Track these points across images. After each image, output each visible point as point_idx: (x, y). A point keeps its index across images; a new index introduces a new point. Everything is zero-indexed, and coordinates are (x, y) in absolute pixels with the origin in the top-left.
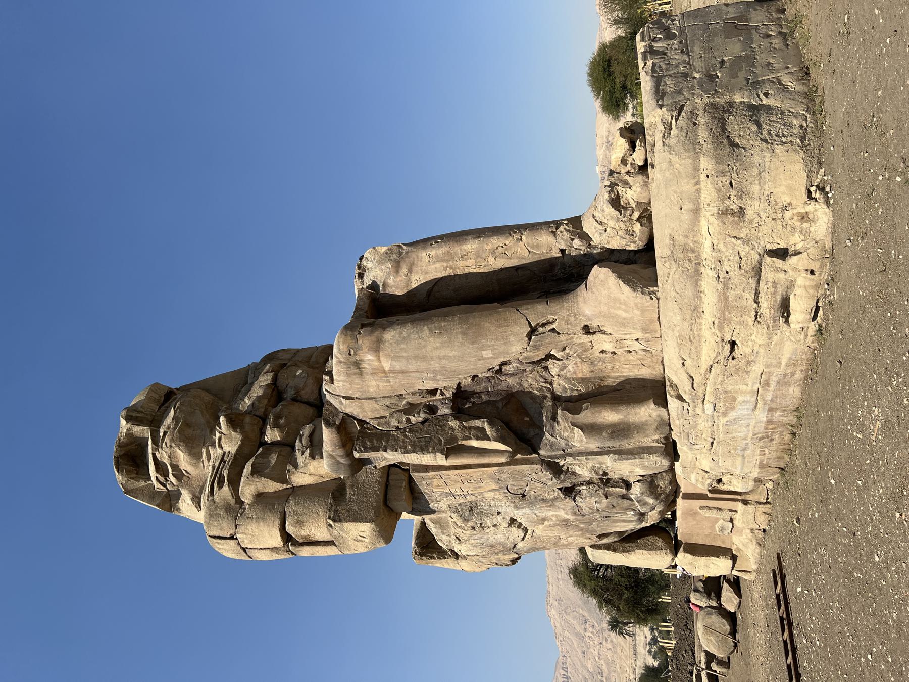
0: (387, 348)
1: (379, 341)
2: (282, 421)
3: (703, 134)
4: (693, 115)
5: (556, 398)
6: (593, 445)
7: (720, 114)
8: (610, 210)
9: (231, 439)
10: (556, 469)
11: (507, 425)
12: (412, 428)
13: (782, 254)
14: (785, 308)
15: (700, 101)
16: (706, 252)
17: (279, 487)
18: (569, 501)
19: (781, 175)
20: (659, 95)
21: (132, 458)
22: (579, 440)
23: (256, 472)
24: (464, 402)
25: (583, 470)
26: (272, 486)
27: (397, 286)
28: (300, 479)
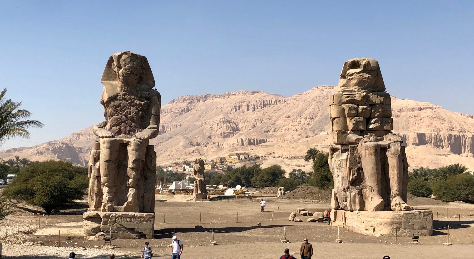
0: (370, 156)
1: (372, 155)
2: (364, 111)
3: (396, 220)
4: (400, 219)
5: (362, 189)
6: (352, 197)
7: (400, 223)
8: (395, 203)
9: (360, 97)
10: (348, 188)
11: (356, 180)
12: (355, 158)
13: (374, 230)
14: (367, 230)
15: (403, 220)
16: (377, 219)
17: (346, 114)
18: (343, 189)
19: (386, 230)
20: (408, 214)
21: (355, 65)
22: (353, 194)
23: (350, 109)
24: (360, 170)
25: (348, 194)
26: (346, 112)
27: (388, 154)
28: (348, 120)
